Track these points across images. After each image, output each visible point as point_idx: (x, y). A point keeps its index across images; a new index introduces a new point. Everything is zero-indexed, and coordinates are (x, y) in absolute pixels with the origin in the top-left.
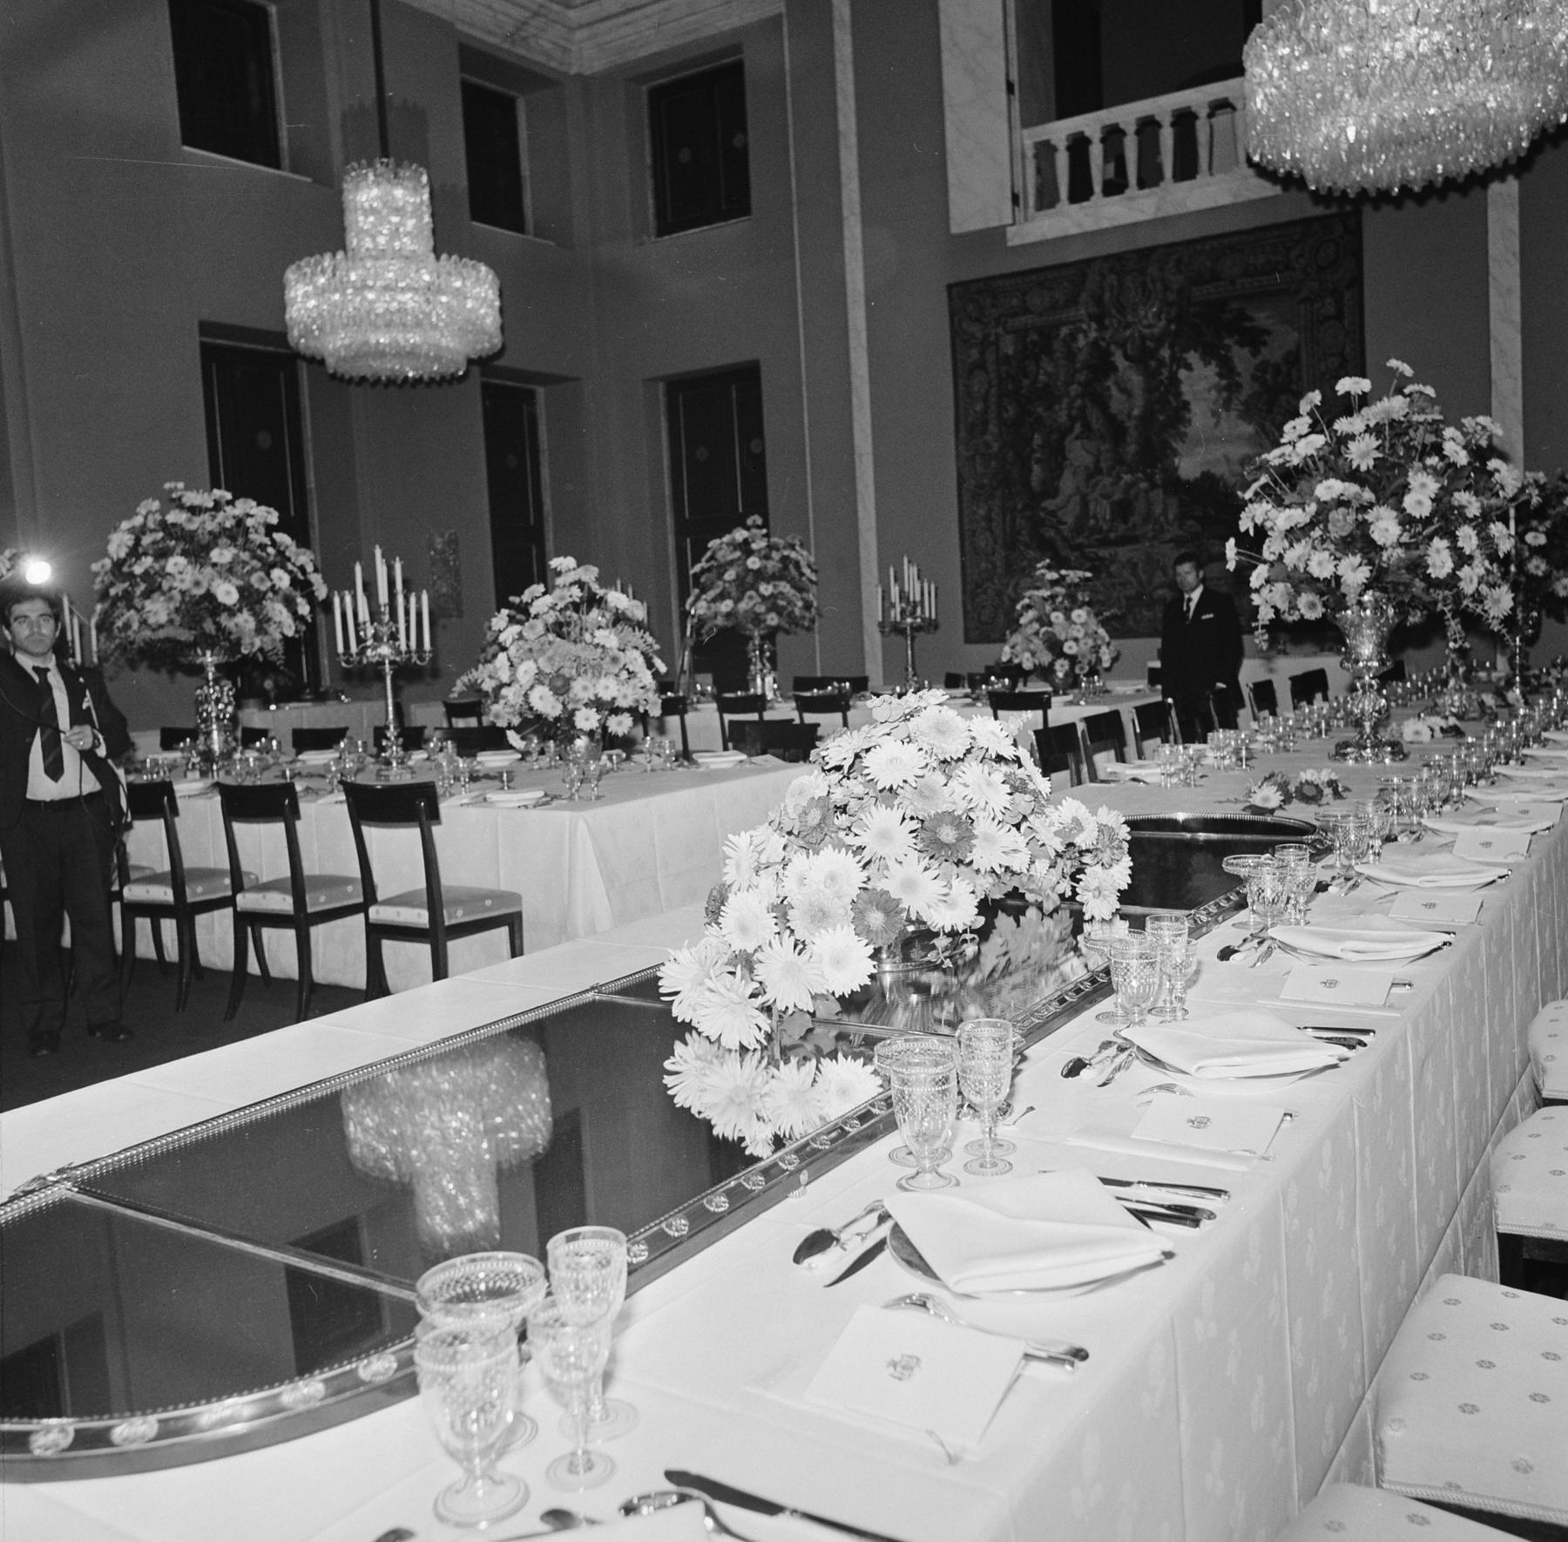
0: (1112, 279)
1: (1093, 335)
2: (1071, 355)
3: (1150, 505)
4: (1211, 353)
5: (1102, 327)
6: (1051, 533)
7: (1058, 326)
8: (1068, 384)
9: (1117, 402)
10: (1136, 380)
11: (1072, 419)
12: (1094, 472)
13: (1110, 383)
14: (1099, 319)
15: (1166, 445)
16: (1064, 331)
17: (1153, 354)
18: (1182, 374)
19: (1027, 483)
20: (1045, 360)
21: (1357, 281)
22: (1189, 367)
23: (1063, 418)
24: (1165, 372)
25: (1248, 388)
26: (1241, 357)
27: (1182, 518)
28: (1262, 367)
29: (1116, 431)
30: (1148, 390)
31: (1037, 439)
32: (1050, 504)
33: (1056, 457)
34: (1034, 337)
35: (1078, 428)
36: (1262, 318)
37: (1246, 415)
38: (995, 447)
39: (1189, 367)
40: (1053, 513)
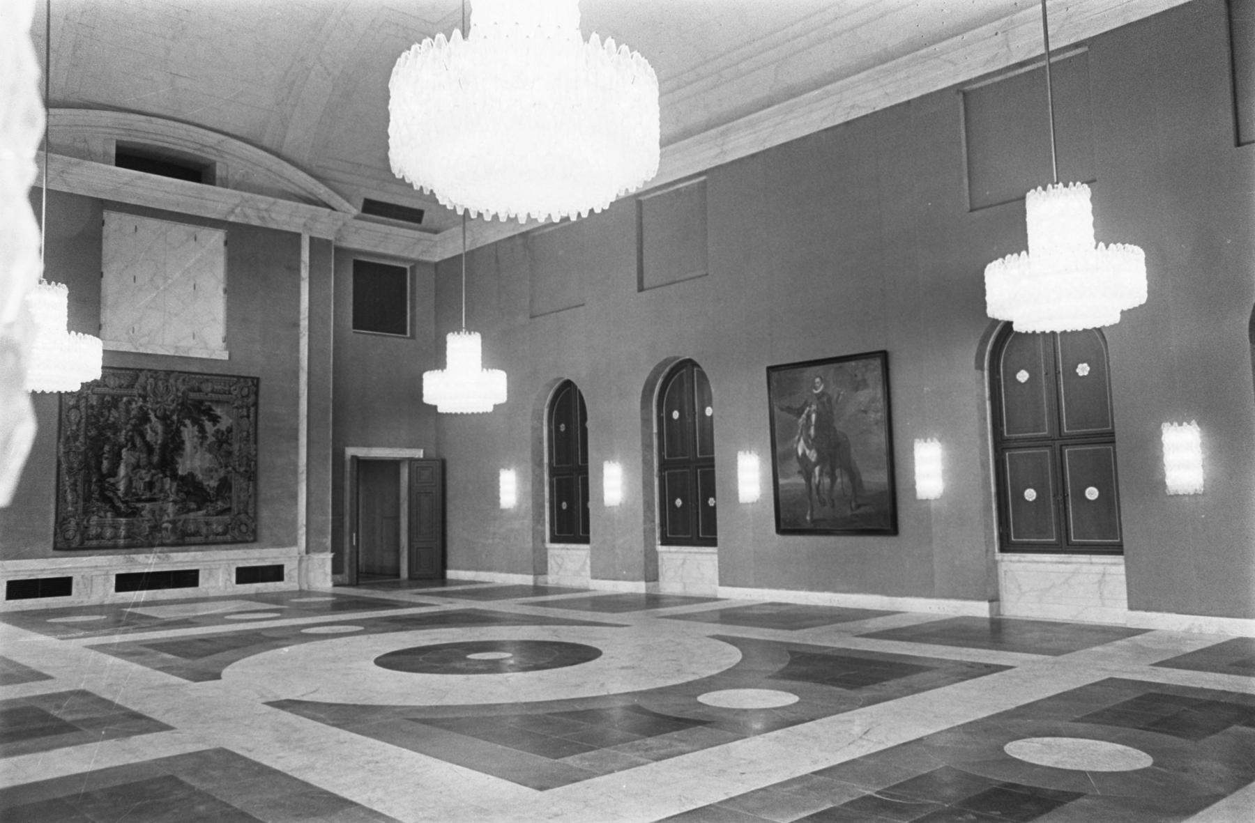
0: (151, 380)
1: (140, 403)
2: (128, 411)
3: (163, 485)
4: (196, 422)
5: (145, 401)
6: (111, 494)
7: (122, 397)
9: (149, 436)
10: (160, 428)
11: (127, 441)
12: (137, 467)
13: (148, 426)
14: (144, 398)
15: (173, 458)
16: (125, 399)
17: (169, 417)
18: (182, 428)
19: (99, 469)
20: (113, 411)
21: (256, 404)
22: (185, 426)
23: (122, 439)
24: (174, 427)
25: (211, 439)
26: (208, 426)
27: (178, 492)
28: (218, 431)
29: (150, 449)
30: (165, 432)
31: (107, 448)
32: (112, 480)
33: (116, 459)
34: (108, 398)
35: (129, 445)
36: (218, 411)
37: (210, 450)
38: (83, 449)
39: (185, 426)
40: (113, 485)
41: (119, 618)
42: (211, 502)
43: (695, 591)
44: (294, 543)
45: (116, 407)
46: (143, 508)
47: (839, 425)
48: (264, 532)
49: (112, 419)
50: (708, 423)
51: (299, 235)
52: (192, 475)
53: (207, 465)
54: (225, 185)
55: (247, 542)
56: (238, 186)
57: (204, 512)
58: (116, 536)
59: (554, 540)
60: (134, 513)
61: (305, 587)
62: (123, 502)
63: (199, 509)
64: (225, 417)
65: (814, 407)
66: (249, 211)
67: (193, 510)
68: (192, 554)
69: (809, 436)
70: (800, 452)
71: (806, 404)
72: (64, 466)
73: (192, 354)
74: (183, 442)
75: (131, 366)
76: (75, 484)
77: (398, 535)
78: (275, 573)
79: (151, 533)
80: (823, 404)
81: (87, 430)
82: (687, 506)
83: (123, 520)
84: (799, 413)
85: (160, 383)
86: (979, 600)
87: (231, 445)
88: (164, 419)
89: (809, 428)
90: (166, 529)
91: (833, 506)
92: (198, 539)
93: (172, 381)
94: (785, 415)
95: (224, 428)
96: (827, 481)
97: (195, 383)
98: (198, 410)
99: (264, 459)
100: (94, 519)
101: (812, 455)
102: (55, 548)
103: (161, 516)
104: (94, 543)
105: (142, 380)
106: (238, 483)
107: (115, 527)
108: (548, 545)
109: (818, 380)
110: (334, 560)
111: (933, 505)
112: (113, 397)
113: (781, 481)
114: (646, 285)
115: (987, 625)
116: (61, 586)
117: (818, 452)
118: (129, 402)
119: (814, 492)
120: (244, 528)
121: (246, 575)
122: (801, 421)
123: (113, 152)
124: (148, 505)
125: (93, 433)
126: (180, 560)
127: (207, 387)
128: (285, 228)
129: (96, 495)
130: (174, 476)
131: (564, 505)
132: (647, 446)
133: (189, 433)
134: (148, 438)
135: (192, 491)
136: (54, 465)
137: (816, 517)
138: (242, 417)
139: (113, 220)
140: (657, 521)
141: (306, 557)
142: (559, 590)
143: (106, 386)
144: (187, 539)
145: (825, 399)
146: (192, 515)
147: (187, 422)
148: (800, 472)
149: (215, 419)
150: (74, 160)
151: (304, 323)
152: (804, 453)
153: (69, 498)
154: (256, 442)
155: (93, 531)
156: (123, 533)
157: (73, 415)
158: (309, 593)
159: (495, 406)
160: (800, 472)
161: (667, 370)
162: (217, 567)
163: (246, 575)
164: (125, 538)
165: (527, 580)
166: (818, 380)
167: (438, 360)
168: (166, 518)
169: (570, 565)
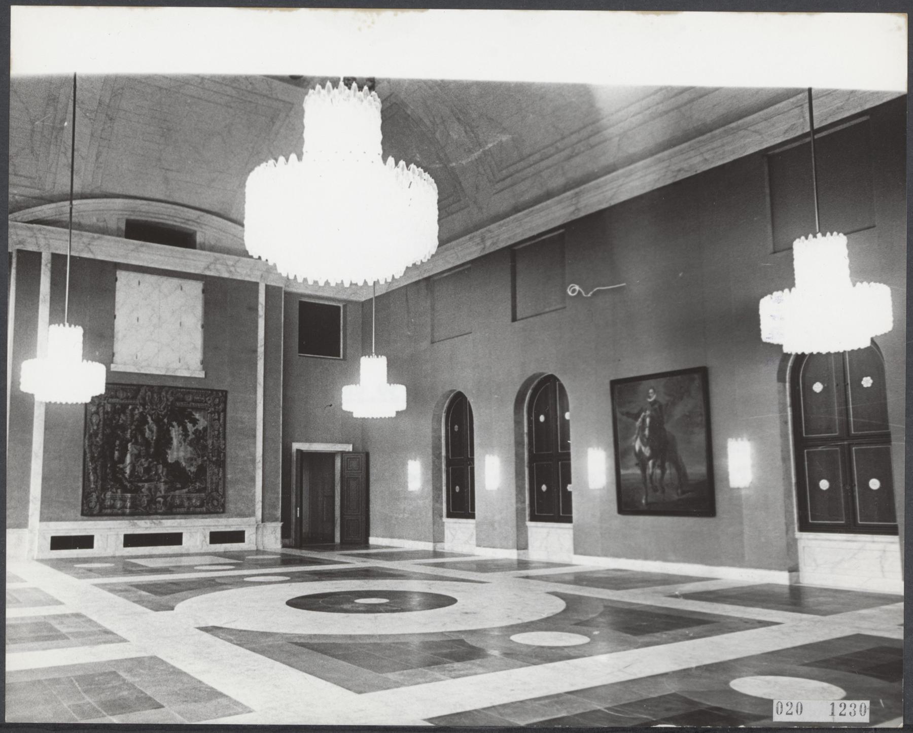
0: (149, 393)
1: (141, 410)
2: (132, 415)
3: (157, 470)
8: (131, 424)
9: (147, 434)
10: (155, 428)
13: (146, 427)
14: (144, 405)
16: (130, 407)
20: (122, 416)
21: (224, 410)
22: (173, 427)
23: (128, 436)
28: (196, 430)
29: (147, 443)
30: (158, 431)
31: (118, 442)
32: (121, 466)
34: (118, 406)
36: (197, 416)
37: (190, 444)
38: (101, 443)
39: (173, 427)
41: (128, 568)
42: (192, 483)
43: (555, 559)
44: (253, 514)
45: (124, 413)
46: (143, 487)
47: (668, 427)
48: (230, 506)
49: (121, 422)
50: (565, 424)
51: (257, 284)
52: (177, 463)
53: (189, 455)
54: (203, 248)
55: (217, 513)
56: (212, 249)
57: (186, 490)
58: (124, 507)
59: (450, 515)
60: (136, 490)
61: (261, 548)
62: (129, 482)
63: (182, 488)
64: (202, 420)
65: (648, 413)
66: (219, 266)
67: (179, 489)
68: (178, 521)
69: (644, 435)
70: (637, 448)
71: (642, 410)
72: (88, 455)
73: (179, 374)
74: (171, 439)
75: (135, 383)
76: (95, 469)
77: (327, 511)
78: (238, 537)
79: (148, 504)
80: (655, 410)
81: (104, 430)
82: (547, 493)
83: (129, 495)
84: (636, 416)
85: (155, 396)
86: (781, 570)
87: (206, 441)
88: (158, 421)
89: (643, 430)
90: (159, 502)
91: (663, 492)
92: (182, 510)
93: (164, 394)
94: (624, 418)
95: (201, 428)
96: (658, 471)
97: (180, 395)
98: (181, 415)
99: (231, 451)
100: (109, 494)
101: (647, 451)
102: (83, 514)
103: (156, 493)
104: (109, 511)
105: (143, 391)
106: (211, 470)
107: (124, 500)
108: (445, 519)
109: (651, 391)
110: (283, 528)
111: (743, 492)
112: (122, 405)
113: (623, 472)
114: (519, 316)
115: (787, 591)
116: (86, 542)
117: (652, 449)
118: (133, 409)
119: (648, 481)
120: (215, 503)
121: (216, 537)
122: (638, 423)
123: (123, 227)
124: (146, 485)
125: (108, 431)
126: (168, 525)
127: (189, 398)
128: (247, 279)
129: (110, 477)
130: (165, 463)
131: (457, 489)
132: (519, 443)
133: (175, 433)
134: (147, 435)
135: (176, 473)
136: (82, 454)
137: (650, 500)
138: (215, 420)
139: (121, 275)
140: (527, 502)
141: (262, 525)
142: (453, 555)
143: (117, 397)
144: (174, 510)
145: (656, 406)
146: (177, 492)
147: (174, 423)
148: (637, 465)
149: (195, 422)
150: (96, 235)
151: (261, 350)
152: (640, 450)
153: (92, 478)
154: (224, 438)
155: (108, 503)
156: (129, 505)
157: (95, 419)
158: (264, 552)
159: (398, 413)
160: (637, 465)
161: (536, 383)
162: (195, 532)
163: (216, 537)
164: (130, 508)
165: (428, 546)
166: (651, 391)
167: (351, 375)
168: (159, 494)
169: (459, 536)
